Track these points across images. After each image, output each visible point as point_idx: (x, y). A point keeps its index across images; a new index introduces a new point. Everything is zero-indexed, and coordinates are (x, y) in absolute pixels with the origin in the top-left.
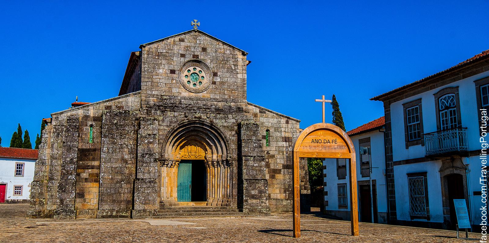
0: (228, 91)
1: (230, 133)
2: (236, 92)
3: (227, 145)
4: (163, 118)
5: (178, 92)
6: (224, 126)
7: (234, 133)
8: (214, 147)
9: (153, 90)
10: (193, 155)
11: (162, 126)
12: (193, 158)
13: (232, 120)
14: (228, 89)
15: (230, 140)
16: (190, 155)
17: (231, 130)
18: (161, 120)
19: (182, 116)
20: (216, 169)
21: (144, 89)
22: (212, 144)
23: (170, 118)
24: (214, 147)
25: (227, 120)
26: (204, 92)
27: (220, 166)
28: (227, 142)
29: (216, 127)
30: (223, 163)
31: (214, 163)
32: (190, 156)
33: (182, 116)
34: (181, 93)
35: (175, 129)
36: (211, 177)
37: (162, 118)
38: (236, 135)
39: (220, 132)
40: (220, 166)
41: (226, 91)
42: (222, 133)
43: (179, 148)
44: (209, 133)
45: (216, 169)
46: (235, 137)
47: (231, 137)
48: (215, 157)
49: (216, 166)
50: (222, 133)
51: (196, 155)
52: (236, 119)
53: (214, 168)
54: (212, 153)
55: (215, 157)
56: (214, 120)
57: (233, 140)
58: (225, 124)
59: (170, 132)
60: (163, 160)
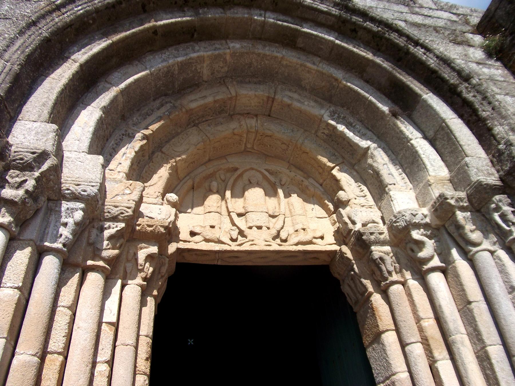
8: (381, 160)
10: (259, 228)
20: (437, 280)
22: (364, 143)
24: (381, 160)
27: (466, 248)
29: (373, 20)
30: (488, 226)
31: (416, 235)
36: (417, 350)
40: (466, 248)
45: (437, 280)
49: (436, 262)
53: (422, 277)
54: (379, 190)
55: (404, 200)
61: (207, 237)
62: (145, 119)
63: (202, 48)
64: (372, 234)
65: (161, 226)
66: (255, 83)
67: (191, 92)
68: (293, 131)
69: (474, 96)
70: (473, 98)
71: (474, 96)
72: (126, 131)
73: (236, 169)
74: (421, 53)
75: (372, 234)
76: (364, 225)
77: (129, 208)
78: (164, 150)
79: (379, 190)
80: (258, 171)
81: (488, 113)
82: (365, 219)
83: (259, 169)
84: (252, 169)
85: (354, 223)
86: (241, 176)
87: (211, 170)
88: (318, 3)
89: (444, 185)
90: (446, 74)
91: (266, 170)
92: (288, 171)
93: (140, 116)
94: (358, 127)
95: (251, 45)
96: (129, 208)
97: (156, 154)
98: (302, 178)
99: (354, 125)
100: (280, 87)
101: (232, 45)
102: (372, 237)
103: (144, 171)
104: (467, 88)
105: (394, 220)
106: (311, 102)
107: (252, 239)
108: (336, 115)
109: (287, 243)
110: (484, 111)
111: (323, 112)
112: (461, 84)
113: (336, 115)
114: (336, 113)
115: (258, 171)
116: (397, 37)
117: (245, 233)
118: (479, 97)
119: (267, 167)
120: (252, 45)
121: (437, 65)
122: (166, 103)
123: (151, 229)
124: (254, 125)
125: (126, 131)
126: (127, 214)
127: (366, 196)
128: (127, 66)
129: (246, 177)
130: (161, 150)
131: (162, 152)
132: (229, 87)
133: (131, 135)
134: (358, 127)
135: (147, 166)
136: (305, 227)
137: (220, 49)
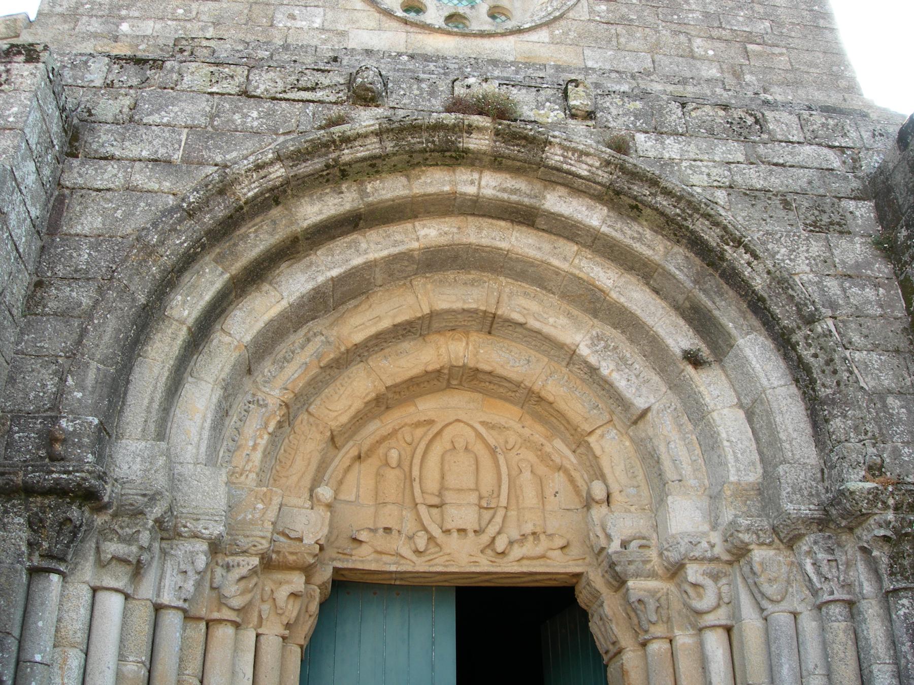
0: (717, 44)
1: (816, 248)
2: (777, 50)
3: (807, 354)
4: (134, 107)
5: (323, 30)
6: (751, 194)
7: (854, 250)
9: (123, 19)
11: (112, 168)
12: (465, 558)
13: (807, 149)
14: (715, 33)
15: (833, 305)
16: (436, 532)
17: (815, 228)
18: (110, 118)
19: (319, 95)
21: (58, 9)
23: (204, 105)
25: (761, 149)
26: (533, 36)
28: (811, 320)
29: (667, 193)
32: (431, 538)
33: (319, 95)
34: (343, 34)
35: (248, 190)
37: (127, 102)
38: (882, 269)
39: (711, 237)
41: (698, 42)
42: (739, 243)
43: (308, 445)
44: (605, 276)
46: (877, 286)
47: (833, 286)
48: (685, 517)
50: (739, 243)
51: (492, 530)
52: (842, 149)
55: (685, 517)
56: (640, 137)
57: (858, 314)
58: (755, 177)
59: (191, 214)
60: (60, 491)
61: (379, 549)
62: (282, 368)
63: (372, 246)
64: (630, 563)
65: (308, 554)
66: (465, 284)
67: (356, 307)
68: (529, 361)
69: (815, 356)
70: (812, 359)
71: (815, 356)
72: (254, 395)
73: (431, 422)
74: (742, 262)
75: (630, 563)
76: (624, 545)
77: (263, 538)
78: (312, 409)
79: (658, 482)
80: (468, 425)
81: (829, 391)
82: (627, 533)
83: (471, 423)
84: (458, 420)
85: (609, 537)
86: (439, 433)
87: (389, 428)
88: (572, 162)
89: (748, 499)
90: (779, 307)
91: (483, 423)
92: (520, 426)
93: (273, 363)
94: (637, 366)
95: (455, 230)
96: (263, 538)
97: (300, 418)
98: (543, 440)
99: (630, 362)
100: (507, 290)
101: (422, 232)
102: (632, 568)
103: (282, 451)
104: (807, 337)
105: (666, 546)
106: (561, 317)
107: (448, 551)
108: (602, 344)
109: (505, 560)
110: (823, 385)
111: (578, 338)
112: (799, 328)
113: (602, 344)
114: (602, 339)
115: (468, 425)
116: (705, 228)
117: (439, 541)
118: (821, 360)
119: (485, 418)
120: (459, 228)
121: (766, 288)
122: (315, 335)
123: (294, 557)
124: (461, 354)
125: (254, 395)
126: (260, 547)
127: (638, 486)
128: (254, 294)
129: (447, 434)
130: (307, 410)
131: (310, 413)
132: (420, 297)
133: (261, 402)
134: (637, 366)
135: (287, 440)
136: (538, 530)
137: (402, 242)
